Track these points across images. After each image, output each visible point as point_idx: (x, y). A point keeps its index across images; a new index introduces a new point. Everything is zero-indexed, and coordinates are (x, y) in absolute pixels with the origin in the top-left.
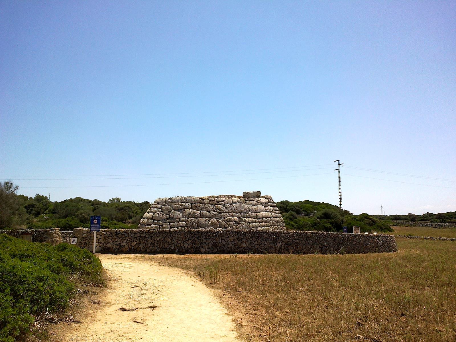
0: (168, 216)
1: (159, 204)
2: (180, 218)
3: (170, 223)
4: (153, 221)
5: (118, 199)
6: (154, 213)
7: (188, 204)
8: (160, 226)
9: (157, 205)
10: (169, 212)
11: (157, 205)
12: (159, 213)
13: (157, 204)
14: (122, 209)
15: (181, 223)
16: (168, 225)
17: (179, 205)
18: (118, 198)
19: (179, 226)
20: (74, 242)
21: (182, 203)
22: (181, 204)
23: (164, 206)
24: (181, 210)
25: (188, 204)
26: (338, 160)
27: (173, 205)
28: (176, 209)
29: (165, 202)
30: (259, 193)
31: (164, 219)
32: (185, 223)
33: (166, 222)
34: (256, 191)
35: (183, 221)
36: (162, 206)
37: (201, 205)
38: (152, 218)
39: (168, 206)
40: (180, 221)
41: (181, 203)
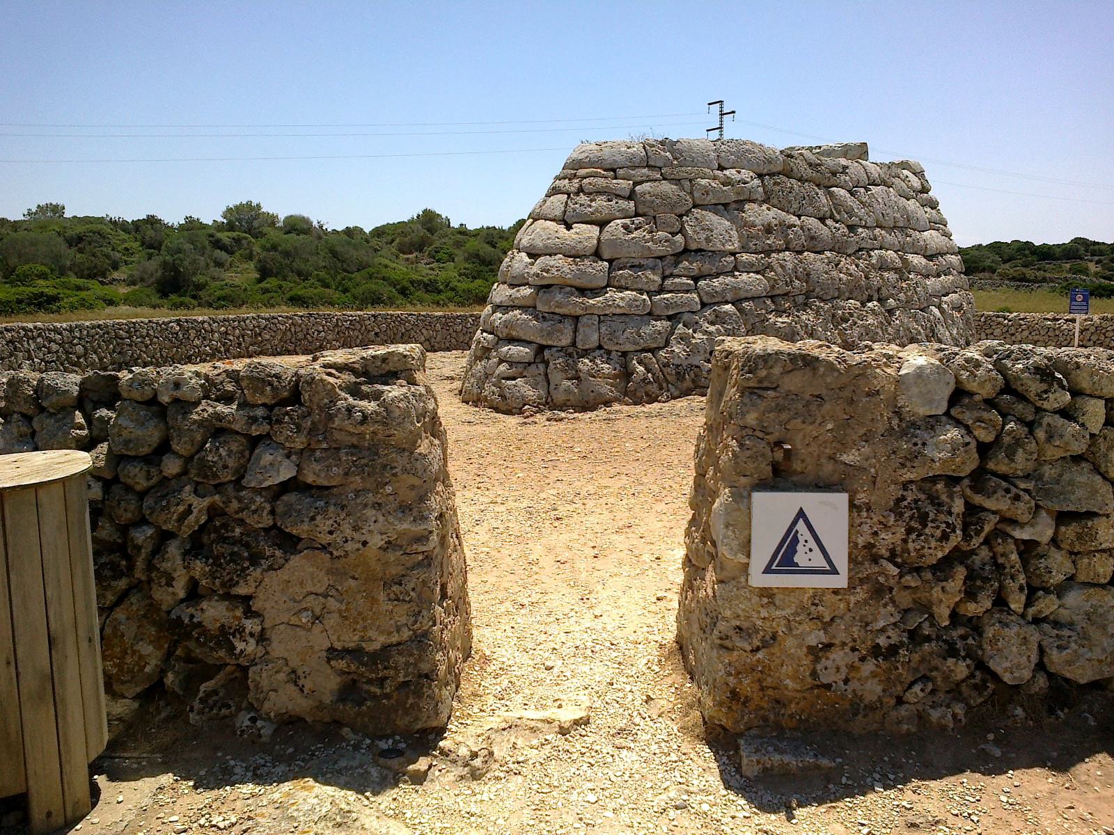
0: (679, 238)
2: (733, 254)
3: (696, 279)
5: (57, 210)
6: (602, 224)
10: (681, 216)
12: (627, 221)
14: (80, 239)
15: (744, 276)
16: (687, 292)
17: (715, 178)
18: (57, 206)
19: (743, 297)
20: (801, 559)
21: (727, 172)
23: (646, 187)
24: (725, 205)
26: (721, 102)
27: (690, 181)
31: (661, 258)
32: (759, 276)
34: (858, 141)
36: (636, 184)
38: (597, 254)
39: (666, 187)
40: (736, 268)
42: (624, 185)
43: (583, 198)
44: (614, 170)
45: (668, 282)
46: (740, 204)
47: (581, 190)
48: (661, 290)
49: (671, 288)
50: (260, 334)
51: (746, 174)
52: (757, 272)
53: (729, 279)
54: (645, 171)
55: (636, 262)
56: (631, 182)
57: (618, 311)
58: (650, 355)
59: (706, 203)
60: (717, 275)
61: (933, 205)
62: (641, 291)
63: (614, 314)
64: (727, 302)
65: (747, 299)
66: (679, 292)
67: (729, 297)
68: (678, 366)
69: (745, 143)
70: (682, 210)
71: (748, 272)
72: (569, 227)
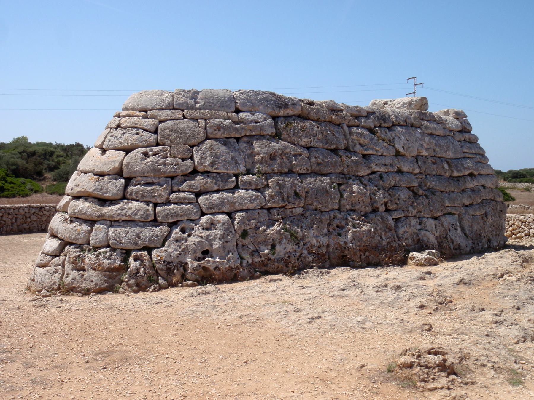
0: (188, 162)
1: (146, 112)
2: (237, 176)
3: (198, 195)
4: (126, 185)
5: (25, 139)
6: (127, 151)
7: (261, 118)
8: (156, 205)
9: (138, 116)
10: (192, 147)
11: (138, 116)
13: (138, 113)
14: (33, 154)
17: (229, 118)
19: (239, 208)
21: (241, 115)
22: (234, 115)
23: (168, 123)
25: (261, 118)
27: (206, 120)
28: (219, 134)
29: (171, 107)
30: (424, 101)
31: (173, 178)
33: (179, 191)
35: (248, 186)
36: (160, 122)
37: (308, 123)
38: (119, 173)
39: (185, 124)
40: (237, 187)
41: (237, 111)
42: (149, 123)
43: (119, 132)
44: (146, 112)
45: (173, 196)
46: (251, 138)
47: (119, 126)
48: (168, 202)
49: (176, 201)
50: (30, 217)
51: (258, 116)
52: (257, 190)
53: (230, 195)
54: (169, 112)
55: (150, 180)
56: (157, 121)
57: (125, 218)
58: (145, 253)
59: (218, 136)
60: (217, 191)
61: (473, 141)
62: (148, 203)
63: (123, 221)
64: (223, 213)
65: (241, 210)
66: (182, 203)
67: (226, 209)
68: (169, 263)
69: (264, 93)
70: (193, 142)
71: (247, 190)
72: (104, 151)
